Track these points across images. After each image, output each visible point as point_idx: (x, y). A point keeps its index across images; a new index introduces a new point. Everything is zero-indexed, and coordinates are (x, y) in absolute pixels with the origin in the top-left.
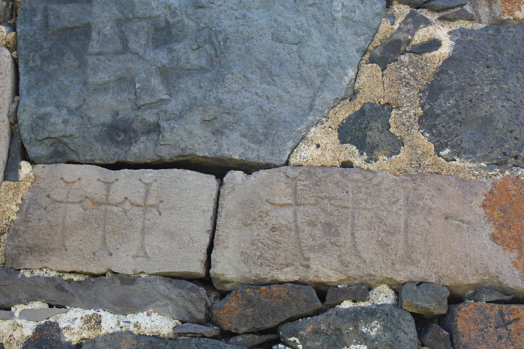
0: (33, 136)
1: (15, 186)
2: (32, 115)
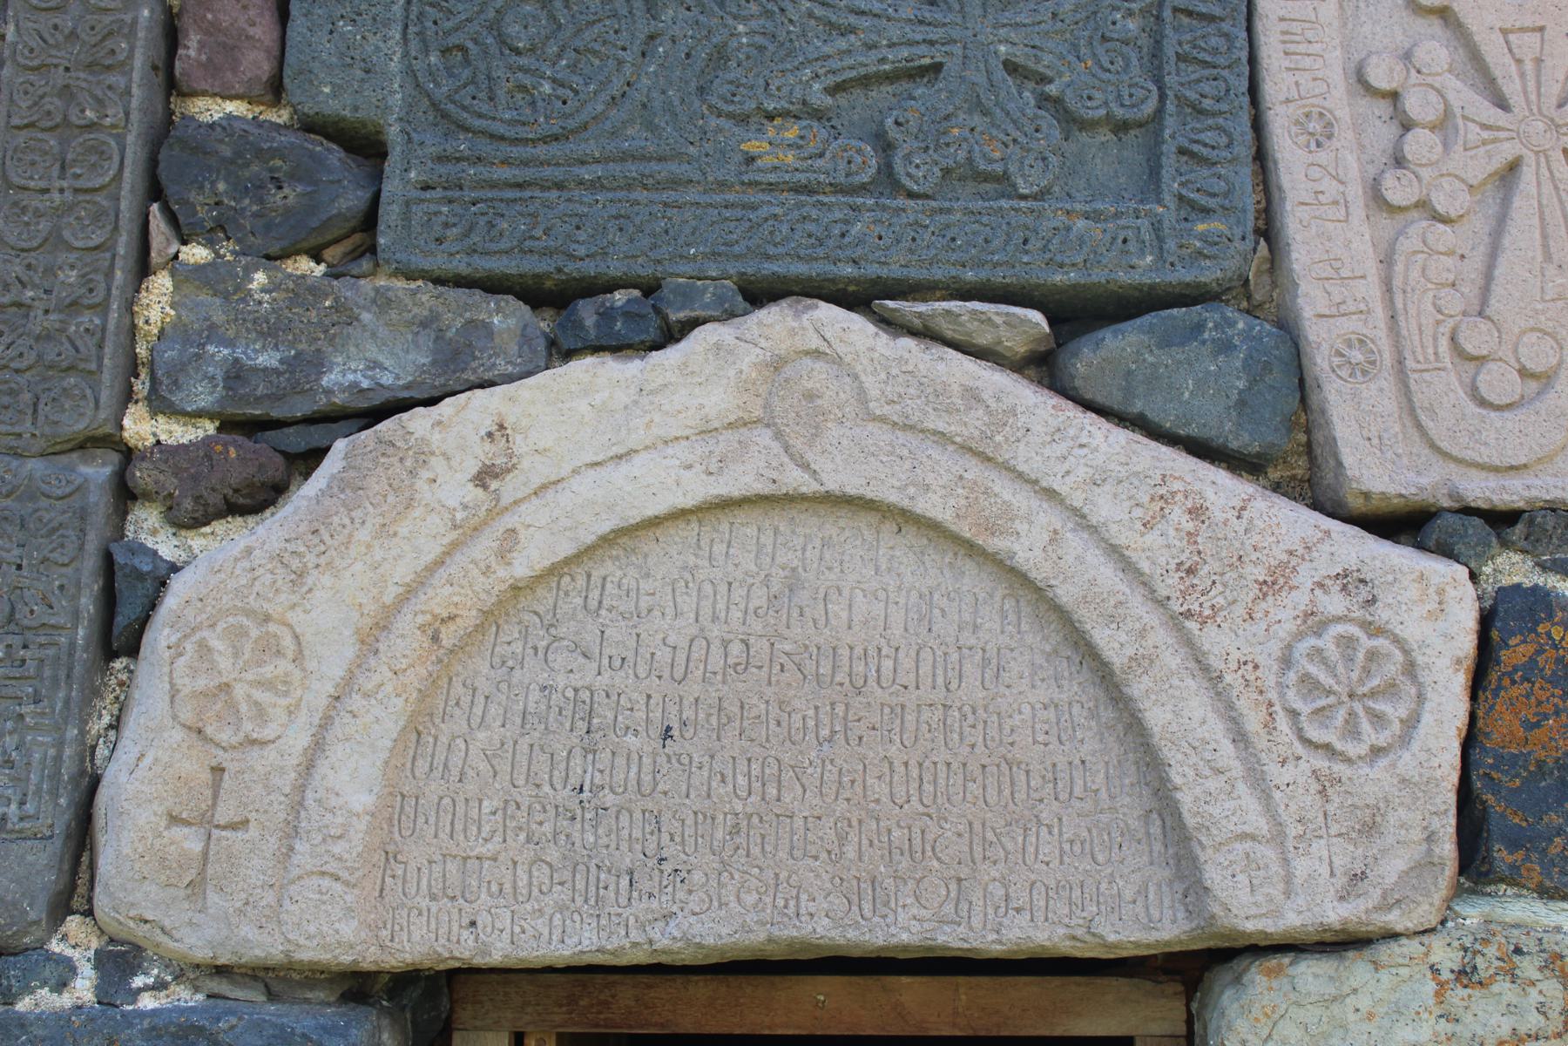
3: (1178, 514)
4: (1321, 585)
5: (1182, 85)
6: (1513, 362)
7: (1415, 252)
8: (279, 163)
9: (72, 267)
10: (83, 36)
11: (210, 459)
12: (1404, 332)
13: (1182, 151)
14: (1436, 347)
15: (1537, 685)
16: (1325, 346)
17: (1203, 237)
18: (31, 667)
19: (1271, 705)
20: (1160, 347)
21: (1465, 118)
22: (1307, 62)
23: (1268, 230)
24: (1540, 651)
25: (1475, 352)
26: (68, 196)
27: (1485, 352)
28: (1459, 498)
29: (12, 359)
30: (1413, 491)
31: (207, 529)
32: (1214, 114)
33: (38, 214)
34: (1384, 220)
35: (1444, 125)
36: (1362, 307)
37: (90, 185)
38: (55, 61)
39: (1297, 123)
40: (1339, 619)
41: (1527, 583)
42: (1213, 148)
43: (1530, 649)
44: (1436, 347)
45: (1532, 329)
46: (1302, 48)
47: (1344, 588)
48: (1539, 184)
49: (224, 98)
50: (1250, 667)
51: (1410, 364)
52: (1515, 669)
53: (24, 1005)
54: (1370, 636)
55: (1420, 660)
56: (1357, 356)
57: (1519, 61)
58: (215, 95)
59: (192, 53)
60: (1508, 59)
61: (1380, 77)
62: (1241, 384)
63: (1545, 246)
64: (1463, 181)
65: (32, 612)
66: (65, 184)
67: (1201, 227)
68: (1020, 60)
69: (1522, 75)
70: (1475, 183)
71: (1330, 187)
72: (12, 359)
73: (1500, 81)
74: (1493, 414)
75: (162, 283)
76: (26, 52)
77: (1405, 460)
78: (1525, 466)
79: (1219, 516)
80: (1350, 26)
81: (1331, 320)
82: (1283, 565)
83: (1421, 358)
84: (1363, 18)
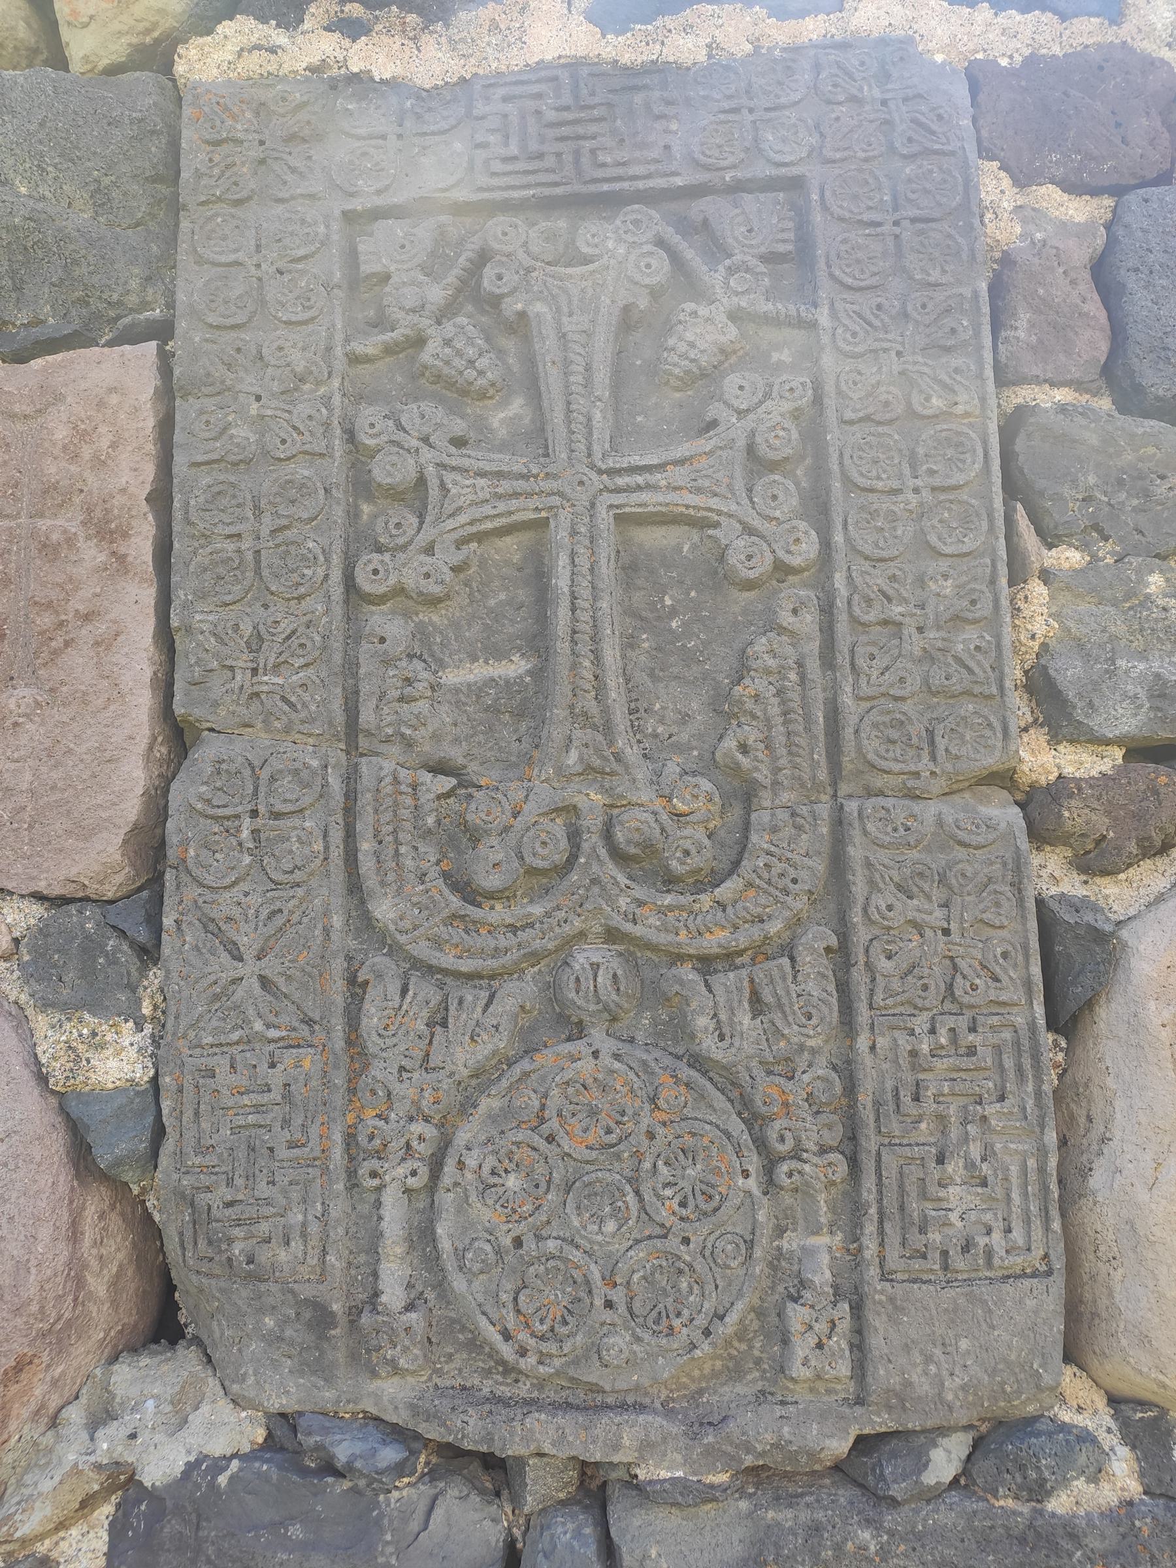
8: (1151, 450)
9: (945, 577)
10: (915, 315)
11: (1156, 793)
18: (986, 1056)
26: (926, 494)
29: (892, 685)
31: (1122, 876)
33: (892, 517)
37: (952, 482)
38: (886, 345)
49: (1052, 385)
53: (1059, 1504)
58: (1046, 381)
59: (1022, 334)
65: (974, 987)
66: (919, 482)
72: (892, 685)
75: (1038, 590)
76: (848, 336)
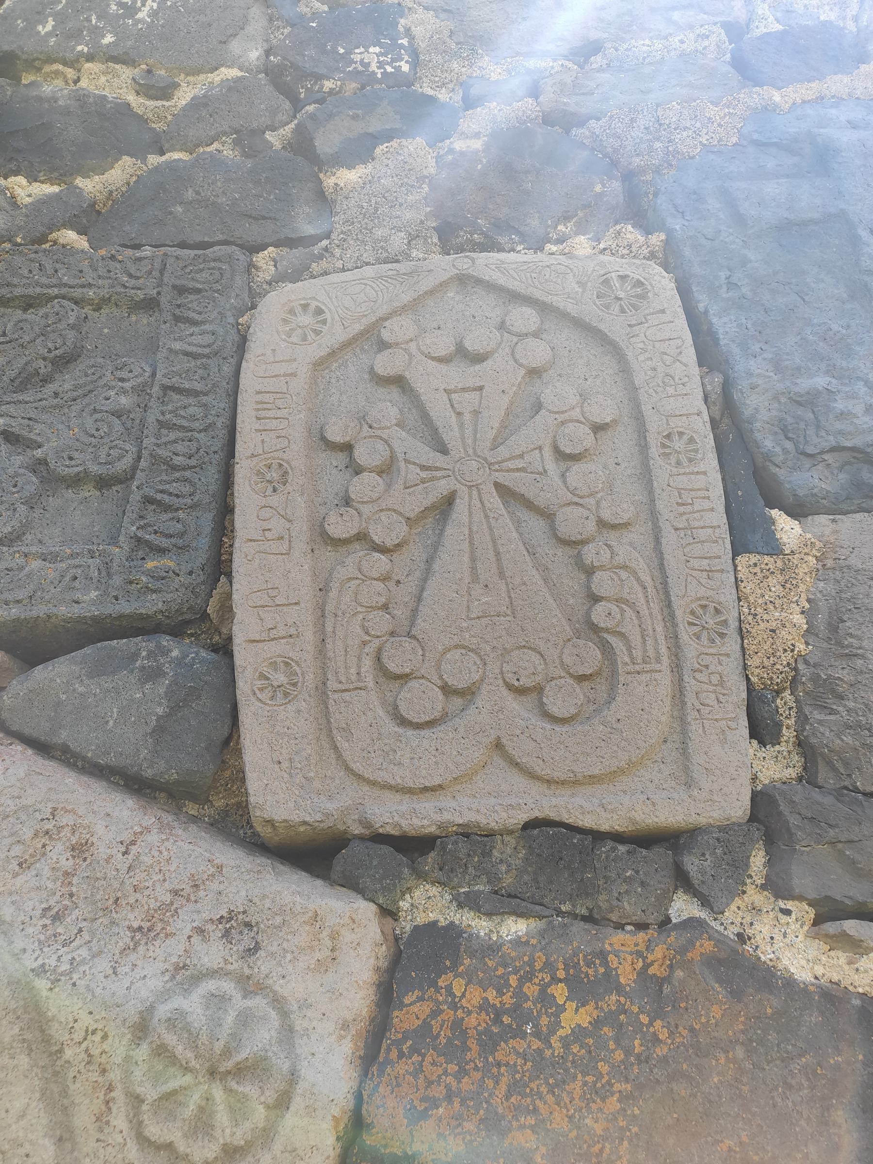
0: (789, 445)
1: (780, 564)
2: (775, 398)
3: (59, 854)
4: (200, 931)
5: (158, 445)
6: (435, 678)
7: (350, 579)
12: (330, 654)
13: (148, 500)
14: (359, 666)
15: (428, 1059)
16: (250, 669)
17: (149, 574)
19: (111, 1088)
20: (90, 676)
21: (406, 461)
22: (274, 424)
23: (220, 567)
24: (435, 1013)
25: (399, 671)
27: (408, 670)
28: (367, 824)
30: (319, 817)
32: (184, 469)
34: (327, 554)
35: (386, 470)
36: (292, 631)
39: (258, 473)
40: (213, 973)
41: (443, 923)
42: (177, 496)
43: (423, 1009)
44: (359, 666)
45: (456, 647)
46: (271, 414)
47: (227, 934)
48: (470, 513)
50: (97, 1038)
51: (332, 684)
52: (405, 1038)
54: (247, 994)
55: (299, 1024)
56: (280, 678)
57: (459, 414)
60: (450, 412)
61: (335, 435)
62: (160, 711)
63: (473, 569)
64: (401, 514)
67: (150, 564)
68: (16, 430)
69: (461, 426)
70: (412, 515)
71: (277, 525)
73: (441, 430)
74: (410, 733)
77: (317, 784)
78: (440, 787)
79: (101, 851)
80: (321, 397)
81: (261, 645)
82: (165, 907)
83: (343, 679)
84: (333, 390)
